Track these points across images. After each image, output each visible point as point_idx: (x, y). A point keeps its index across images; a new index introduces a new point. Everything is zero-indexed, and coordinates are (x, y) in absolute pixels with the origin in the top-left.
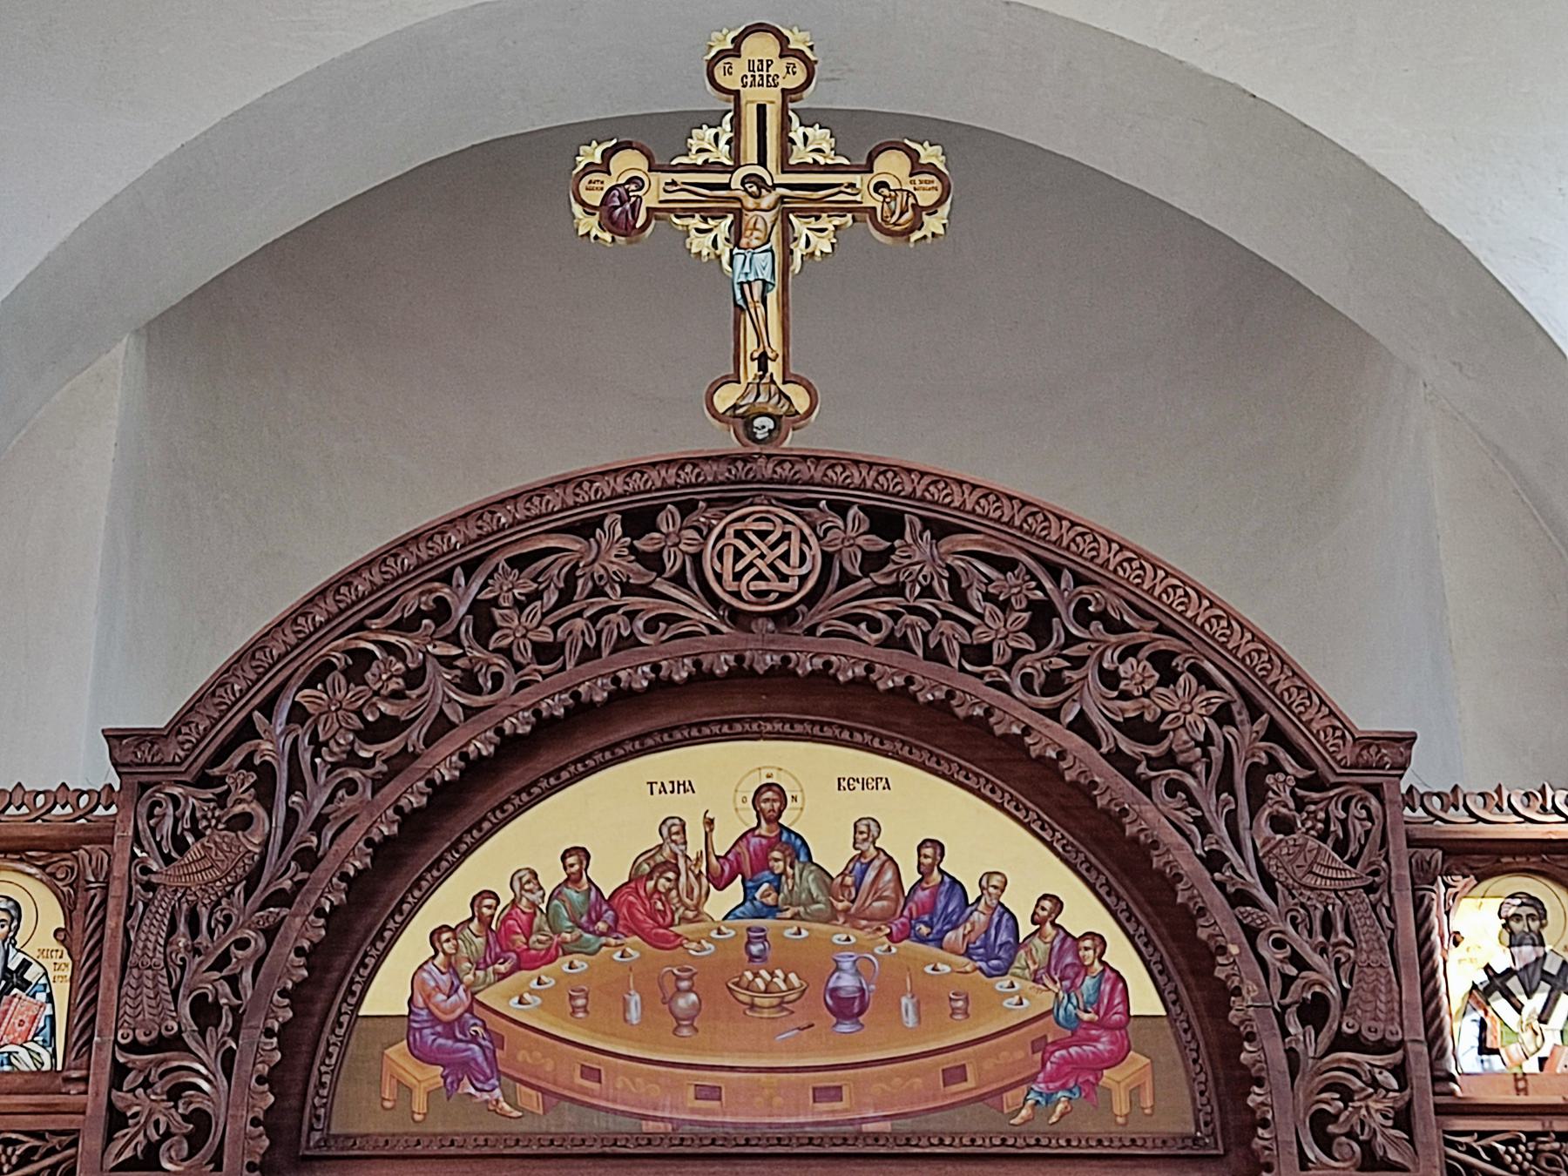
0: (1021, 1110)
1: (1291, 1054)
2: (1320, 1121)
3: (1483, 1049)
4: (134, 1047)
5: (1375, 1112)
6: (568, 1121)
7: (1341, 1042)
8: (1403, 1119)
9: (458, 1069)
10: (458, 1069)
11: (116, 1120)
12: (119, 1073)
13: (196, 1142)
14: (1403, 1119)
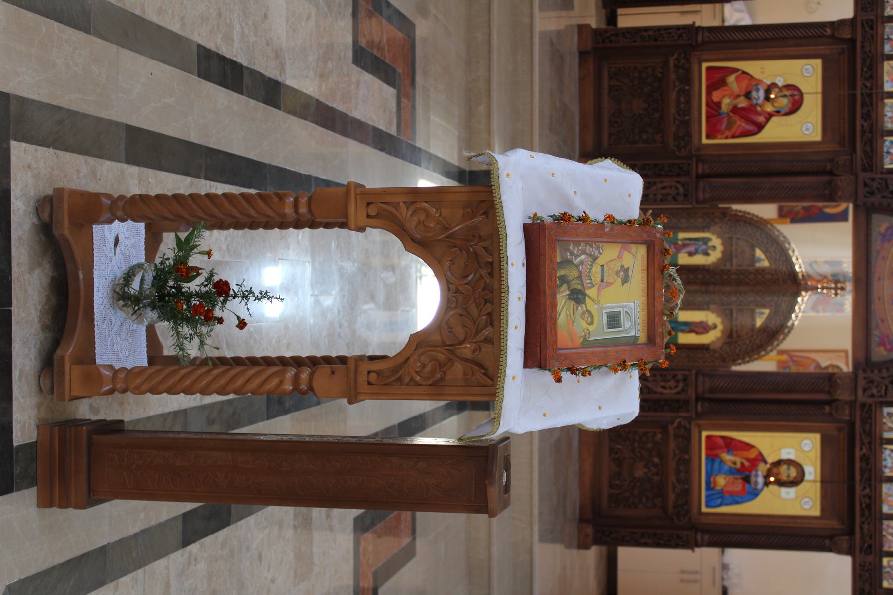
0: (875, 332)
1: (884, 378)
2: (872, 382)
3: (888, 413)
4: (886, 181)
5: (874, 391)
6: (874, 254)
7: (886, 387)
8: (872, 396)
9: (884, 235)
10: (884, 235)
11: (873, 180)
12: (882, 179)
13: (869, 193)
14: (872, 396)
